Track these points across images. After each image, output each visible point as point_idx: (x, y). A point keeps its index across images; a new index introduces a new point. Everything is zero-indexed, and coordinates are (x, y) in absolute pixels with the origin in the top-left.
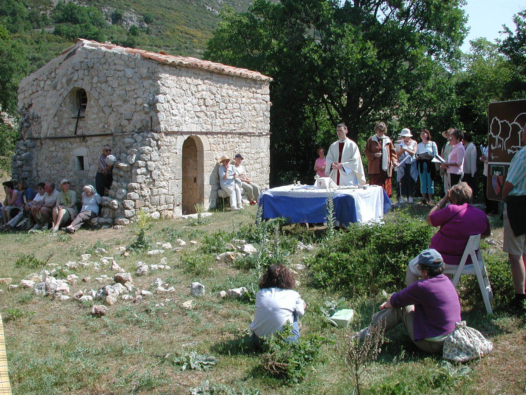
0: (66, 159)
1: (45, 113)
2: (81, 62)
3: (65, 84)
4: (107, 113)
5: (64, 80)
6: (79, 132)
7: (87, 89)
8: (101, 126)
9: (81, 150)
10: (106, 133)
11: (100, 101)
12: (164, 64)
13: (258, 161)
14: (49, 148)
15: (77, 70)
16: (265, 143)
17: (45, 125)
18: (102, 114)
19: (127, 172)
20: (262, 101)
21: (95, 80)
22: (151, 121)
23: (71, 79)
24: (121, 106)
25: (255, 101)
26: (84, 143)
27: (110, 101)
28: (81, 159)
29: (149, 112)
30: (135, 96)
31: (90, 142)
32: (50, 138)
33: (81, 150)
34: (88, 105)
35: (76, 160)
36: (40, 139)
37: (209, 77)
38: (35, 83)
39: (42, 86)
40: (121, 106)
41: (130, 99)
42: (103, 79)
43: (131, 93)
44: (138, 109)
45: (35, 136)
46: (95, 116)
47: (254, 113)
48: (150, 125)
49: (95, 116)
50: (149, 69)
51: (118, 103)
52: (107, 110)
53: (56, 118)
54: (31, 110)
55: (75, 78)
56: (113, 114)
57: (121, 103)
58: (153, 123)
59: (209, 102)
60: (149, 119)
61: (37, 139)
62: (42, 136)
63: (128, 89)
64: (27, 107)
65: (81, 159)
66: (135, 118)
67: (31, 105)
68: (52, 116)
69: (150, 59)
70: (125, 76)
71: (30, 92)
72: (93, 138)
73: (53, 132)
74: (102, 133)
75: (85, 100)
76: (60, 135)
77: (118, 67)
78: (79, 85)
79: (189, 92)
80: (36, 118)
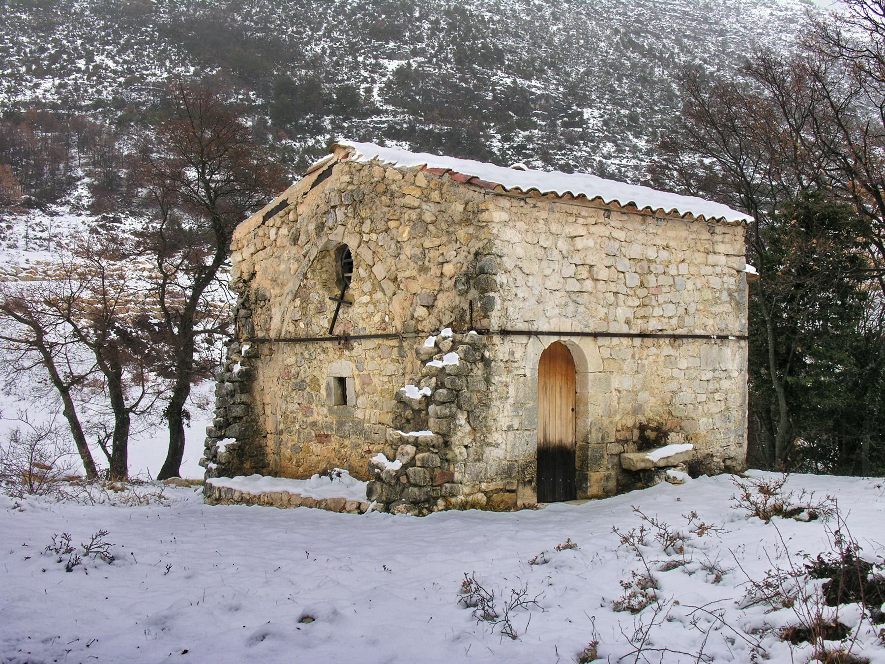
0: (315, 381)
1: (277, 291)
2: (340, 191)
3: (314, 234)
4: (389, 293)
5: (312, 227)
6: (338, 330)
7: (352, 243)
8: (377, 318)
9: (342, 366)
10: (388, 331)
11: (374, 269)
12: (501, 192)
13: (717, 396)
14: (288, 357)
15: (334, 207)
16: (735, 359)
17: (276, 313)
18: (379, 295)
19: (420, 411)
20: (726, 270)
21: (366, 227)
22: (471, 309)
23: (323, 224)
24: (414, 278)
25: (710, 270)
26: (347, 353)
27: (393, 268)
28: (342, 381)
29: (467, 292)
30: (441, 260)
31: (358, 348)
32: (285, 340)
33: (342, 366)
34: (353, 275)
35: (333, 384)
36: (269, 341)
37: (602, 219)
38: (261, 233)
39: (273, 237)
40: (414, 278)
41: (431, 265)
42: (381, 226)
43: (432, 254)
44: (446, 286)
45: (260, 334)
46: (366, 299)
47: (708, 294)
48: (468, 318)
49: (366, 299)
50: (466, 204)
51: (407, 274)
52: (389, 287)
53: (298, 302)
54: (254, 284)
55: (330, 224)
56: (401, 295)
57: (414, 273)
58: (474, 315)
59: (603, 274)
60: (466, 306)
61: (263, 341)
62: (273, 335)
63: (427, 244)
64: (246, 277)
65: (342, 381)
66: (439, 304)
67: (253, 275)
68: (290, 297)
69: (471, 181)
70: (420, 219)
71: (252, 250)
72: (363, 341)
73: (291, 328)
74: (380, 332)
75: (348, 266)
76: (302, 334)
77: (408, 200)
78: (337, 237)
79: (556, 253)
80: (262, 299)
